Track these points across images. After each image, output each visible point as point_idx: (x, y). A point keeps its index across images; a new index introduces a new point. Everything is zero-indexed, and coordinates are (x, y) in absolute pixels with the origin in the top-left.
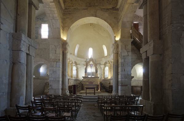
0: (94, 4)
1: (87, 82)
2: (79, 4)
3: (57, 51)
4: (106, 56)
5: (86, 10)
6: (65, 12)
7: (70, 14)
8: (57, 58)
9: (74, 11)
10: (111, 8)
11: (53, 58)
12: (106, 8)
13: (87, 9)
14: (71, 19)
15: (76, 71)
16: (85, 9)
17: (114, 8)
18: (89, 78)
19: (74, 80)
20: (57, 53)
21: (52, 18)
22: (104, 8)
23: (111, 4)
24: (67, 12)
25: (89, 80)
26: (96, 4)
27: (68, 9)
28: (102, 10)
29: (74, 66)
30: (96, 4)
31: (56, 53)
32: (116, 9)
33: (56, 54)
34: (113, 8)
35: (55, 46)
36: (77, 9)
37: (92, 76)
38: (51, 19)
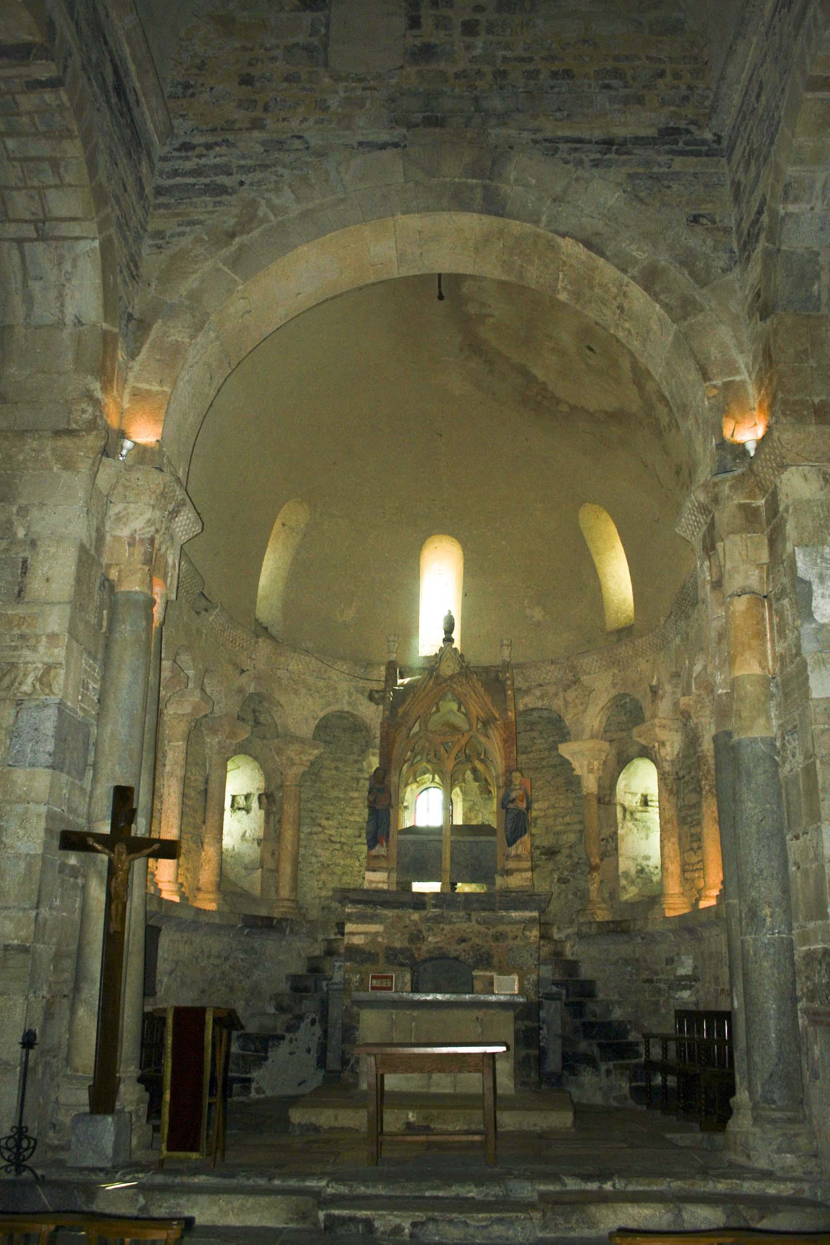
0: (476, 99)
1: (393, 956)
2: (326, 109)
4: (625, 632)
5: (387, 154)
6: (175, 173)
7: (223, 190)
9: (265, 167)
10: (651, 132)
12: (598, 134)
13: (396, 145)
14: (232, 235)
15: (257, 813)
16: (383, 146)
17: (676, 131)
18: (420, 901)
21: (29, 231)
22: (577, 134)
23: (640, 100)
24: (197, 172)
25: (416, 937)
26: (496, 103)
27: (209, 147)
28: (551, 146)
30: (496, 103)
32: (704, 142)
34: (669, 134)
36: (298, 144)
37: (463, 888)
38: (20, 242)
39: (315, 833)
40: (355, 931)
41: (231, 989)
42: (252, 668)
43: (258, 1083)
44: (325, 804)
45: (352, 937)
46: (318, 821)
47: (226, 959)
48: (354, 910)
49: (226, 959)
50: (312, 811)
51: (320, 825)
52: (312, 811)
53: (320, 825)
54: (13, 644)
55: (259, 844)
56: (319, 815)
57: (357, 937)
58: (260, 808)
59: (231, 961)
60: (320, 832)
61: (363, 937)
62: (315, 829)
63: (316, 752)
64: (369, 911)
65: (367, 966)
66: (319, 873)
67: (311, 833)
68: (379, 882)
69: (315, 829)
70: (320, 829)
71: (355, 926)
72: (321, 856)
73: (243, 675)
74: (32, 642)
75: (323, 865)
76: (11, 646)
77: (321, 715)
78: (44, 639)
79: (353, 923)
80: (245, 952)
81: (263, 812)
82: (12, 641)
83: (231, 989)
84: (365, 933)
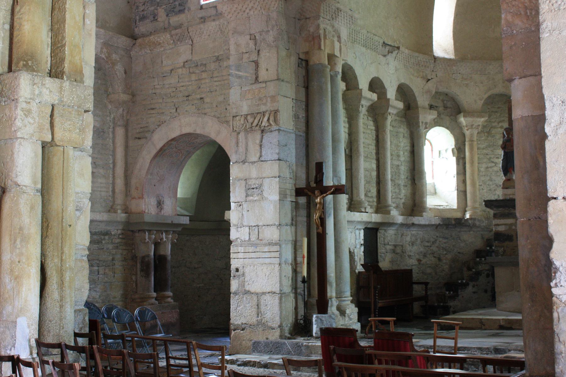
3: (263, 65)
8: (263, 108)
11: (245, 109)
19: (437, 226)
20: (263, 74)
29: (437, 123)
31: (257, 78)
33: (258, 86)
35: (253, 38)
39: (490, 167)
40: (499, 223)
41: (440, 259)
42: (435, 77)
43: (454, 308)
44: (494, 149)
45: (497, 227)
46: (492, 160)
47: (434, 243)
48: (498, 212)
49: (434, 243)
50: (487, 154)
51: (493, 162)
52: (487, 154)
53: (493, 162)
54: (257, 103)
55: (454, 177)
56: (492, 156)
57: (500, 227)
58: (454, 156)
59: (437, 245)
60: (493, 166)
61: (503, 226)
62: (490, 165)
63: (483, 119)
64: (507, 211)
65: (507, 243)
66: (495, 190)
67: (487, 168)
68: (510, 195)
69: (490, 165)
70: (493, 164)
71: (499, 220)
72: (495, 180)
73: (429, 82)
74: (264, 101)
75: (497, 185)
76: (256, 105)
77: (486, 96)
78: (269, 99)
79: (498, 219)
80: (445, 238)
81: (454, 159)
82: (256, 102)
83: (440, 259)
84: (505, 224)
